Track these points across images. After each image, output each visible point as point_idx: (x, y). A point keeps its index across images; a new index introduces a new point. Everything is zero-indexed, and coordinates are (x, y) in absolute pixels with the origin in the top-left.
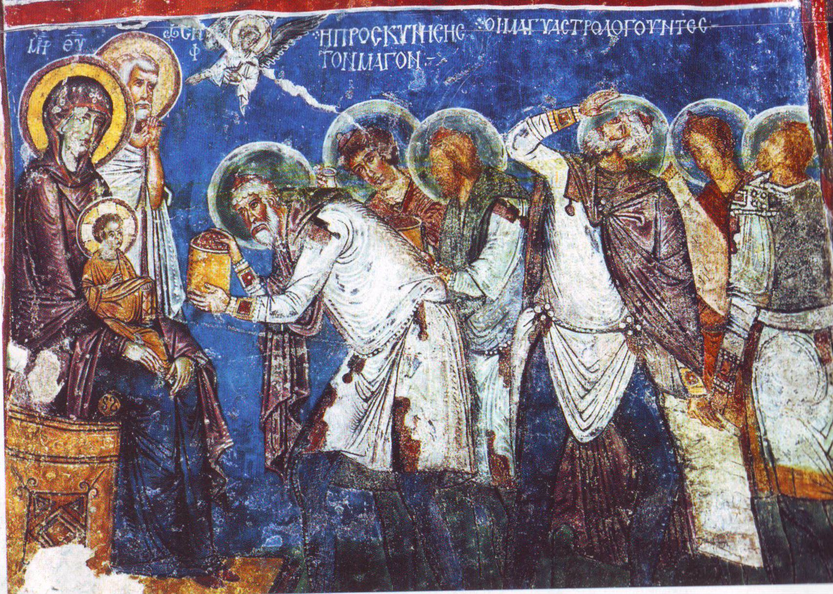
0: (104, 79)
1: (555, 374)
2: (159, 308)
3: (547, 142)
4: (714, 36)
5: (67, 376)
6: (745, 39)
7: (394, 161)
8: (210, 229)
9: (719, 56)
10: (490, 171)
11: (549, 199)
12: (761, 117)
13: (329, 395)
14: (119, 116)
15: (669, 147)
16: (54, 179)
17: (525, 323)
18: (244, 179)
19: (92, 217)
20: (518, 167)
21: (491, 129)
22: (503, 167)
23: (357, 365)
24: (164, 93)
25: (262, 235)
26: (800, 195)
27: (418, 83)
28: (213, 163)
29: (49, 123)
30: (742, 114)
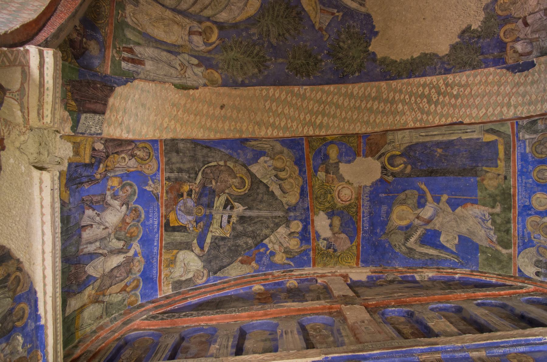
0: (150, 159)
1: (96, 260)
3: (136, 251)
4: (153, 282)
5: (99, 151)
6: (152, 288)
7: (133, 219)
8: (122, 181)
9: (149, 283)
10: (131, 240)
11: (126, 253)
12: (139, 294)
13: (94, 210)
14: (144, 162)
15: (134, 276)
16: (133, 149)
17: (105, 251)
18: (131, 188)
19: (126, 157)
20: (132, 245)
21: (138, 239)
22: (132, 243)
23: (98, 215)
24: (147, 172)
25: (121, 193)
26: (125, 305)
28: (134, 182)
29: (143, 148)
30: (139, 290)
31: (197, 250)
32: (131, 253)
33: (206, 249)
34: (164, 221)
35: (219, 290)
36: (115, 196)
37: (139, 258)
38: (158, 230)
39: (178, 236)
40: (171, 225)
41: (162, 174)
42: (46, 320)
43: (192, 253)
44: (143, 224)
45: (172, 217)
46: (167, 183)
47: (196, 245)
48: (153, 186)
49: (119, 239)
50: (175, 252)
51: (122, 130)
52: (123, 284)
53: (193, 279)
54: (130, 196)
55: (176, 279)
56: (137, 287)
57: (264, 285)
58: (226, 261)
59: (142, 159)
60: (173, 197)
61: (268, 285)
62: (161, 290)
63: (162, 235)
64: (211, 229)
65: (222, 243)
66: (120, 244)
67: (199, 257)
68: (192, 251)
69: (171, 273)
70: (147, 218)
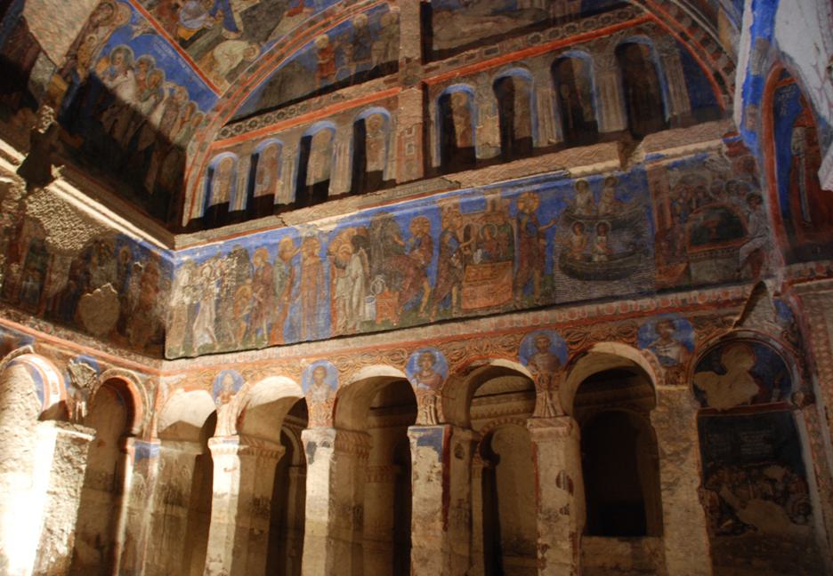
2: (89, 65)
6: (208, 97)
13: (106, 110)
23: (114, 106)
24: (122, 23)
27: (161, 60)
31: (232, 35)
32: (167, 94)
33: (241, 28)
34: (177, 43)
35: (279, 59)
36: (113, 77)
37: (177, 90)
38: (177, 55)
39: (202, 42)
40: (187, 39)
41: (140, 8)
42: (142, 237)
43: (228, 42)
44: (159, 64)
45: (182, 33)
46: (152, 11)
47: (228, 32)
48: (139, 28)
49: (146, 100)
50: (209, 55)
51: (67, 35)
52: (179, 121)
53: (245, 59)
54: (126, 59)
55: (227, 72)
56: (193, 110)
57: (327, 33)
58: (271, 25)
59: (108, 18)
60: (168, 17)
61: (331, 30)
62: (218, 91)
63: (184, 55)
64: (233, 8)
65: (255, 13)
66: (152, 100)
67: (238, 39)
68: (227, 39)
69: (218, 72)
70: (158, 56)
